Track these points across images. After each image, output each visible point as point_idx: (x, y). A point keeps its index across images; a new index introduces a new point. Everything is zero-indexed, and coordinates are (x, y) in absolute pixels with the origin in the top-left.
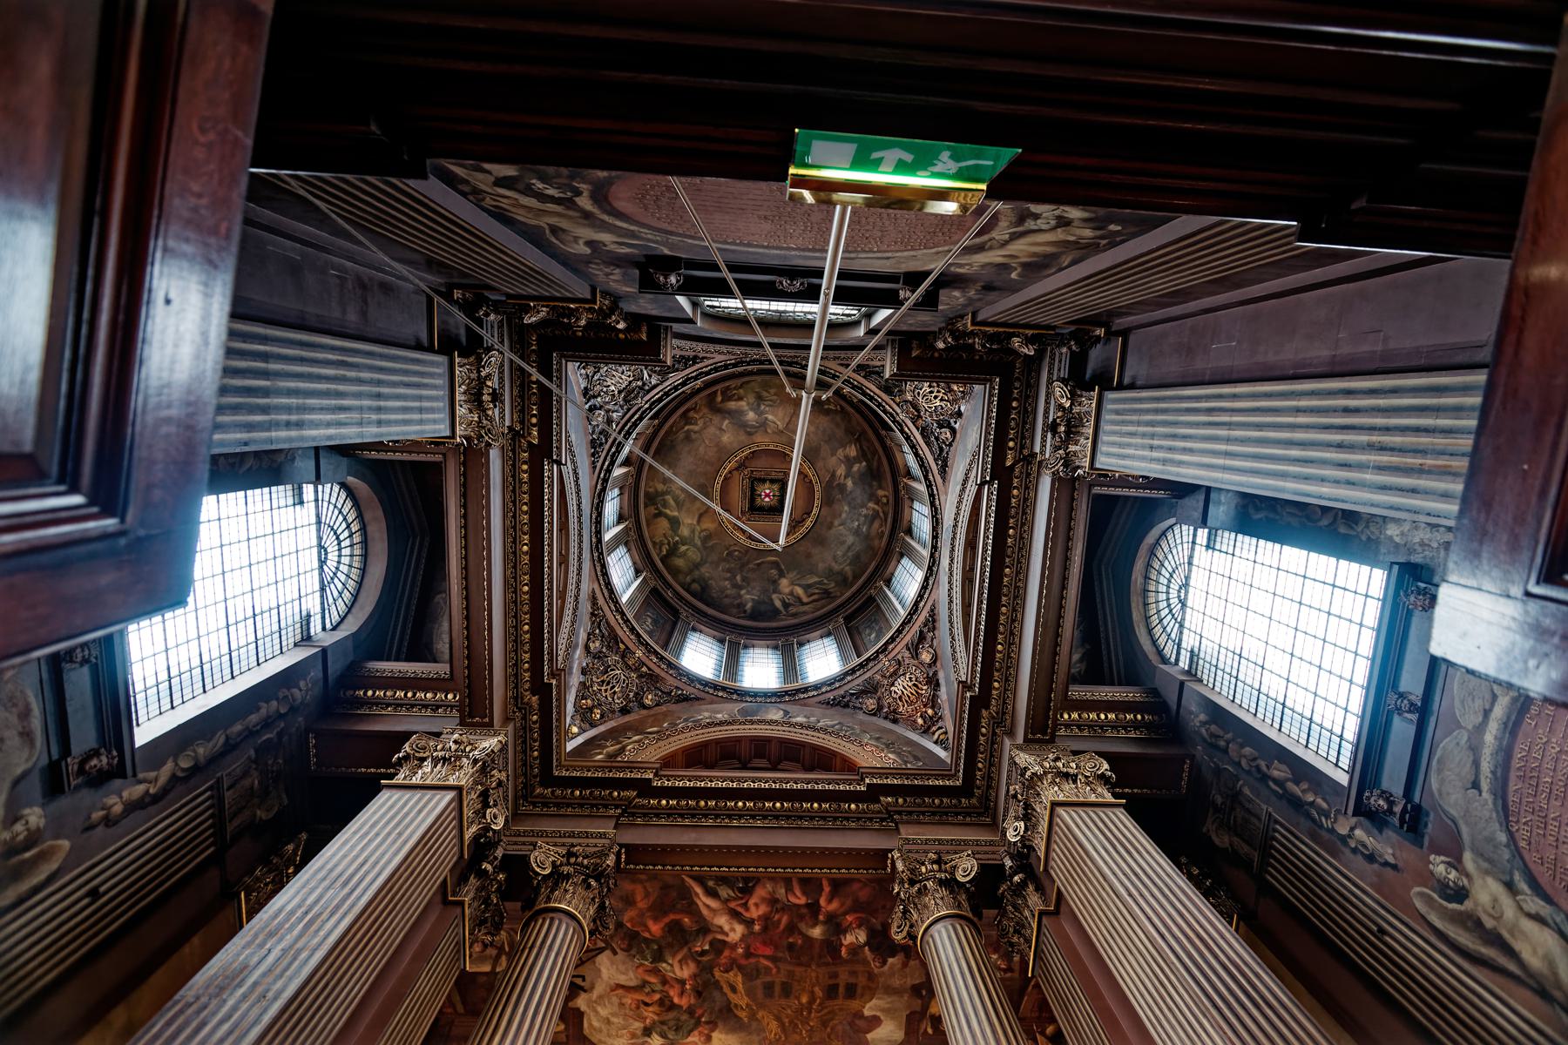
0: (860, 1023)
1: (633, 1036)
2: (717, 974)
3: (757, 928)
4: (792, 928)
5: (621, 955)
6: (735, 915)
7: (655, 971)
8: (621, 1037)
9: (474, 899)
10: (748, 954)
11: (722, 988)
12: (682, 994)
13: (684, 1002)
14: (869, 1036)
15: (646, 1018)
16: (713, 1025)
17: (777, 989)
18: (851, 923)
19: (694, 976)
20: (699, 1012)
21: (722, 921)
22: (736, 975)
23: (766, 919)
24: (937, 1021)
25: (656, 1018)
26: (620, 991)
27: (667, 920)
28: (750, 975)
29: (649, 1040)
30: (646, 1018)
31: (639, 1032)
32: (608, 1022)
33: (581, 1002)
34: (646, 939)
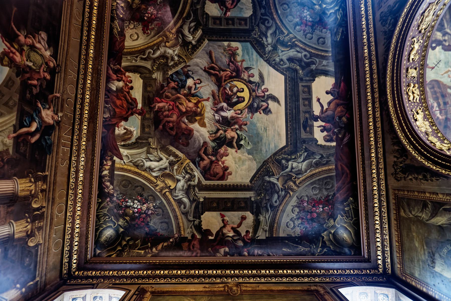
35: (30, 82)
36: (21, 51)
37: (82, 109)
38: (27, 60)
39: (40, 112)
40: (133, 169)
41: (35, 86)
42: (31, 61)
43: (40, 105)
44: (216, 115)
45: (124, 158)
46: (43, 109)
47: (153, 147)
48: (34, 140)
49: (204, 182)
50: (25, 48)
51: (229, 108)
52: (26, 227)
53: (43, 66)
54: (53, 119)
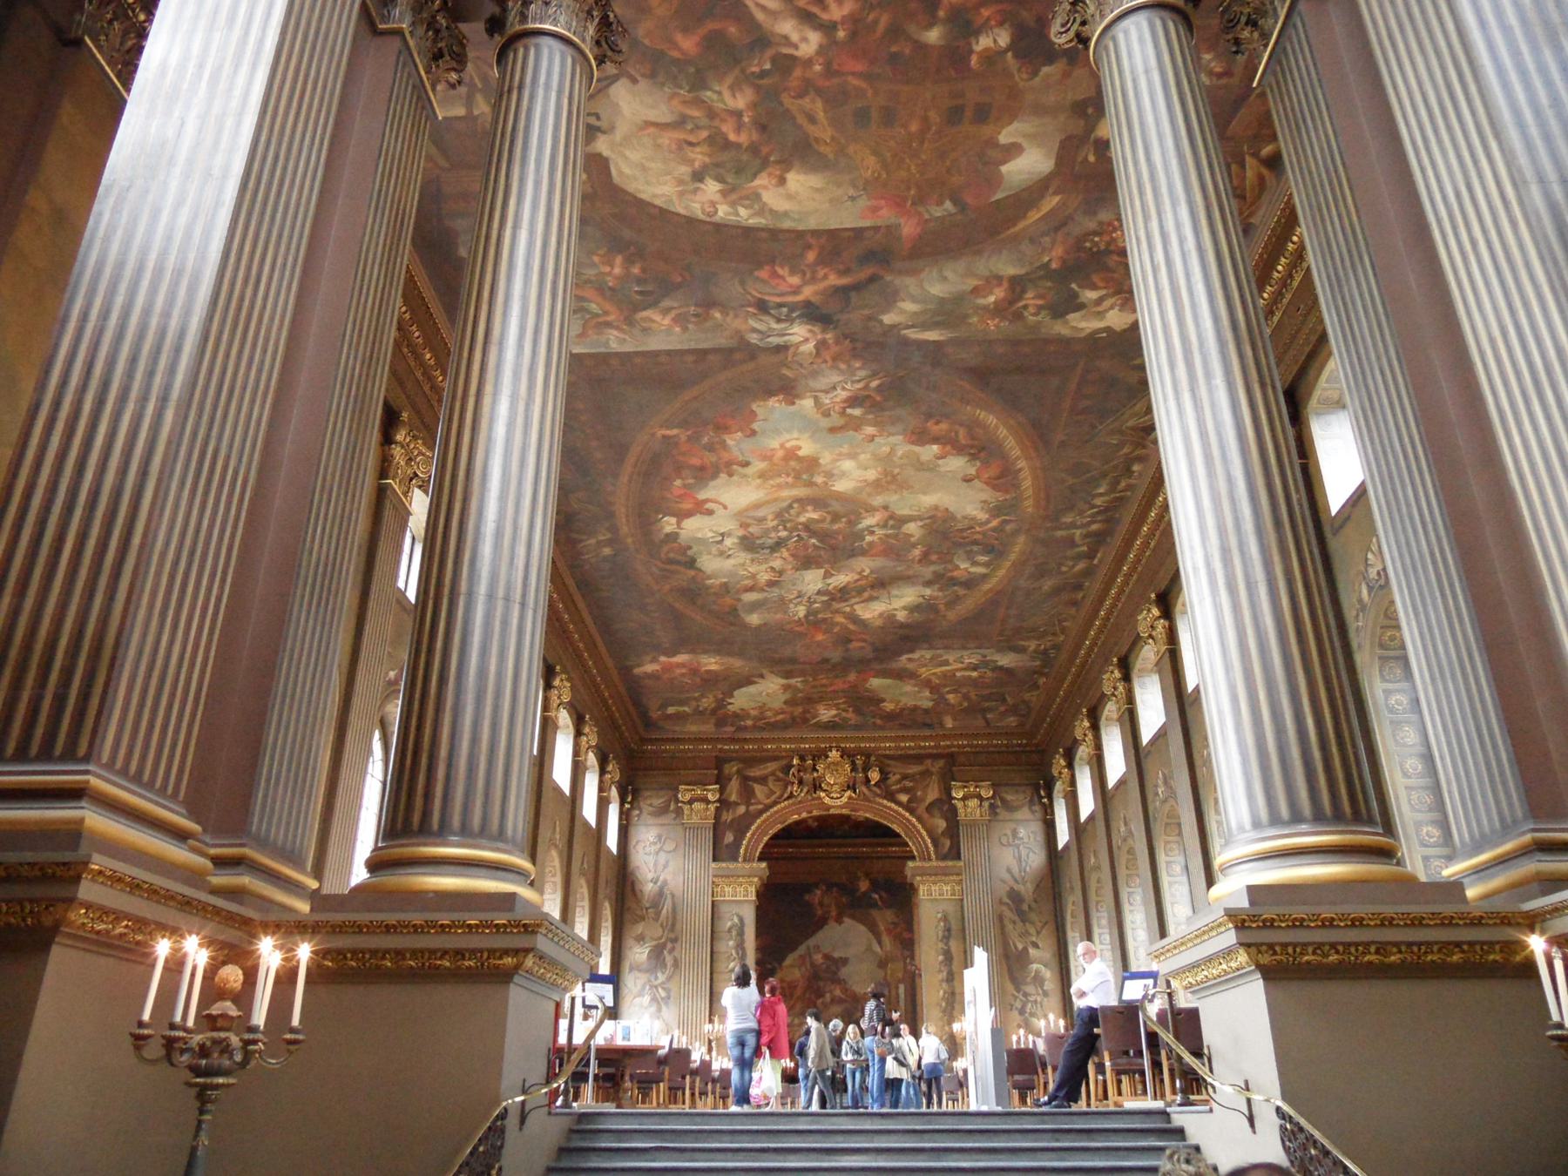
0: (993, 154)
1: (680, 182)
2: (787, 100)
3: (841, 34)
4: (895, 32)
5: (643, 84)
6: (806, 18)
7: (698, 102)
8: (665, 184)
9: (413, 23)
10: (829, 72)
11: (794, 118)
12: (739, 128)
13: (743, 139)
14: (1004, 169)
15: (694, 161)
16: (786, 164)
17: (874, 114)
18: (988, 19)
19: (754, 106)
20: (765, 150)
21: (787, 27)
22: (813, 101)
23: (854, 20)
24: (1103, 146)
25: (707, 160)
26: (652, 130)
27: (703, 31)
28: (835, 100)
29: (702, 186)
30: (694, 161)
31: (687, 178)
32: (644, 169)
33: (602, 145)
34: (676, 62)
36: (829, 912)
48: (884, 894)
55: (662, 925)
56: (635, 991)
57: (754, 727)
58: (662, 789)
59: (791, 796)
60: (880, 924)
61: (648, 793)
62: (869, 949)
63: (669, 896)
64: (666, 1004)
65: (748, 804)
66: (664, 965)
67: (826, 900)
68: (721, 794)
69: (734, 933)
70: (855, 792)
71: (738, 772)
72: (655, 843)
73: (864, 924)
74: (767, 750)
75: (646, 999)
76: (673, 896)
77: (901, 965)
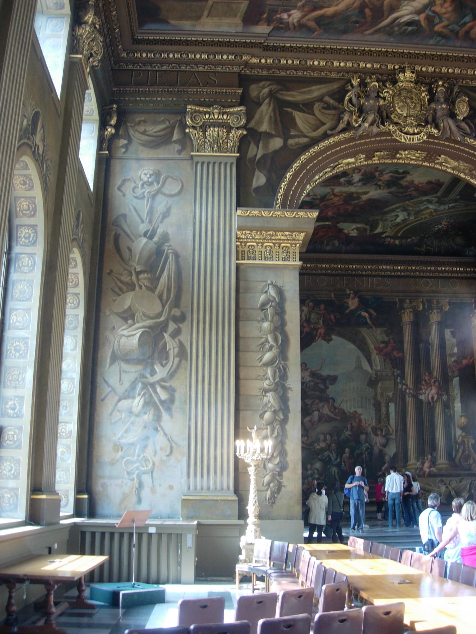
35: (334, 321)
36: (317, 329)
37: (337, 269)
38: (320, 324)
39: (352, 311)
40: (399, 227)
41: (335, 317)
42: (319, 322)
43: (348, 311)
44: (355, 185)
45: (384, 231)
46: (349, 308)
47: (380, 218)
48: (374, 313)
49: (439, 194)
50: (312, 326)
51: (350, 176)
52: (435, 313)
53: (316, 311)
54: (354, 299)
55: (160, 297)
56: (121, 390)
57: (301, 26)
58: (159, 112)
59: (348, 127)
60: (369, 341)
61: (139, 118)
62: (359, 366)
63: (171, 257)
64: (169, 409)
65: (286, 137)
66: (163, 355)
67: (313, 316)
68: (248, 121)
69: (270, 311)
70: (437, 127)
71: (271, 94)
72: (150, 184)
73: (354, 342)
74: (313, 68)
75: (138, 403)
76: (177, 256)
77: (389, 384)
